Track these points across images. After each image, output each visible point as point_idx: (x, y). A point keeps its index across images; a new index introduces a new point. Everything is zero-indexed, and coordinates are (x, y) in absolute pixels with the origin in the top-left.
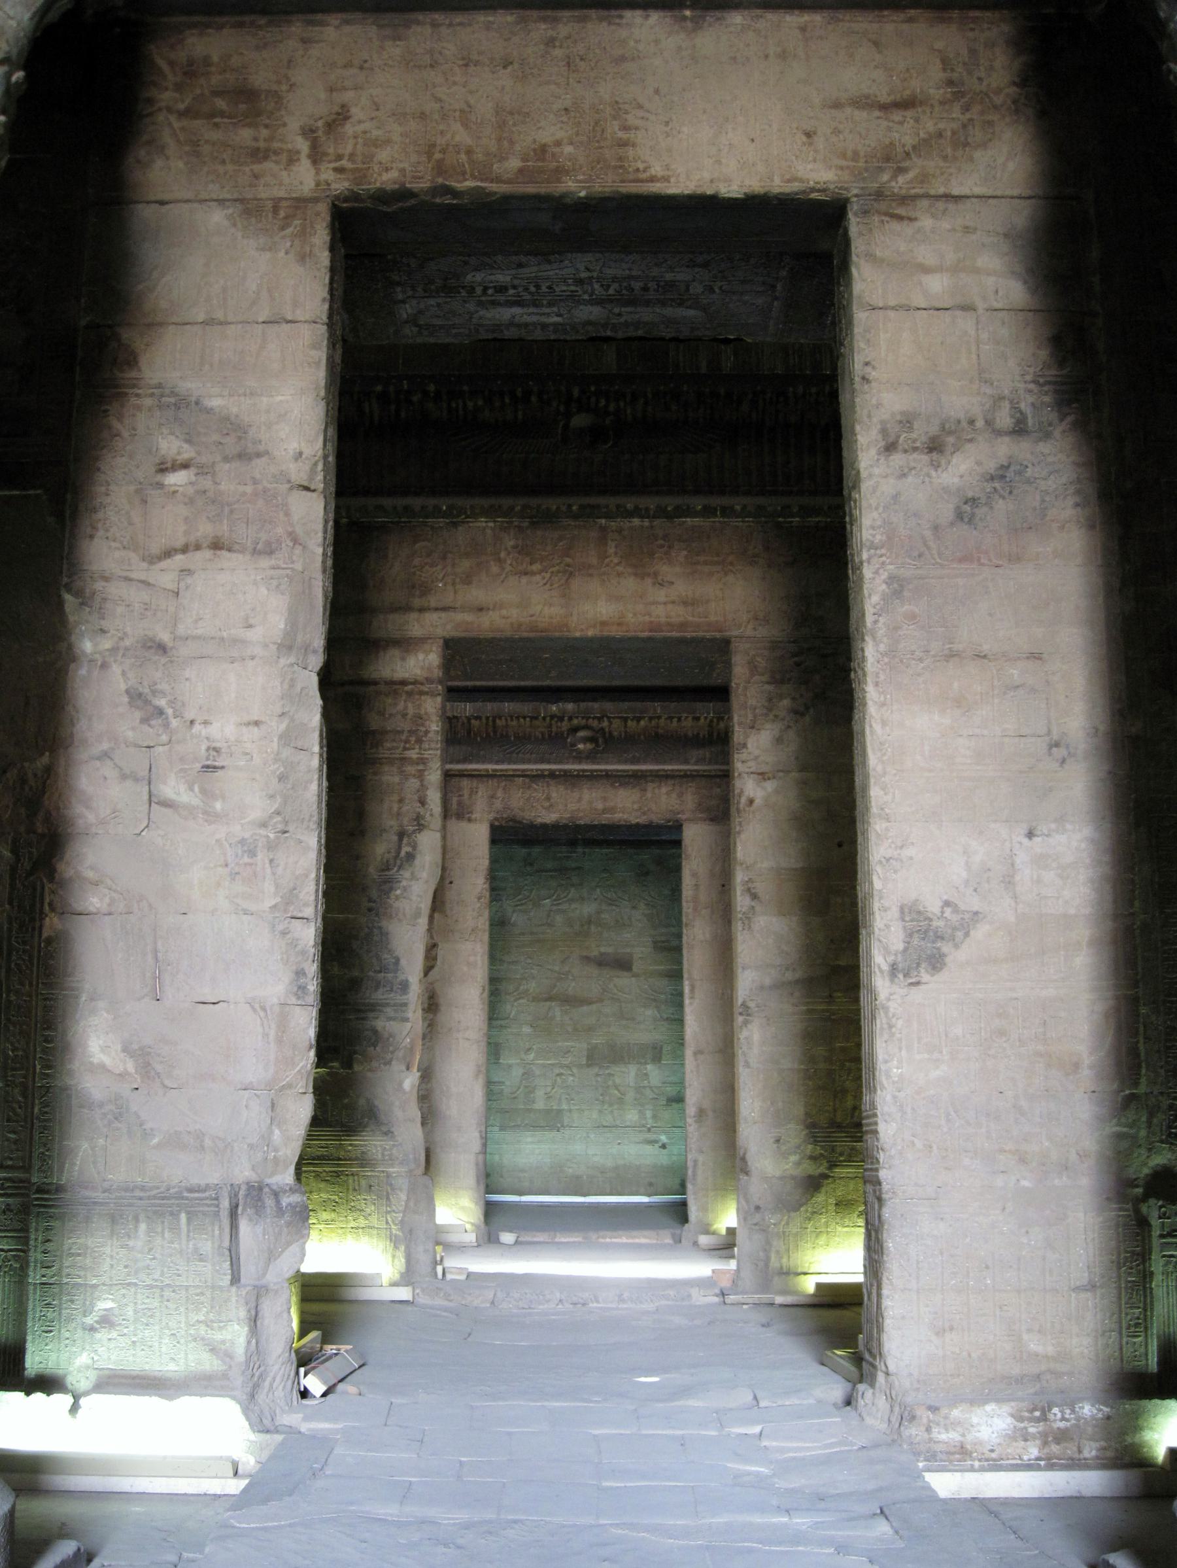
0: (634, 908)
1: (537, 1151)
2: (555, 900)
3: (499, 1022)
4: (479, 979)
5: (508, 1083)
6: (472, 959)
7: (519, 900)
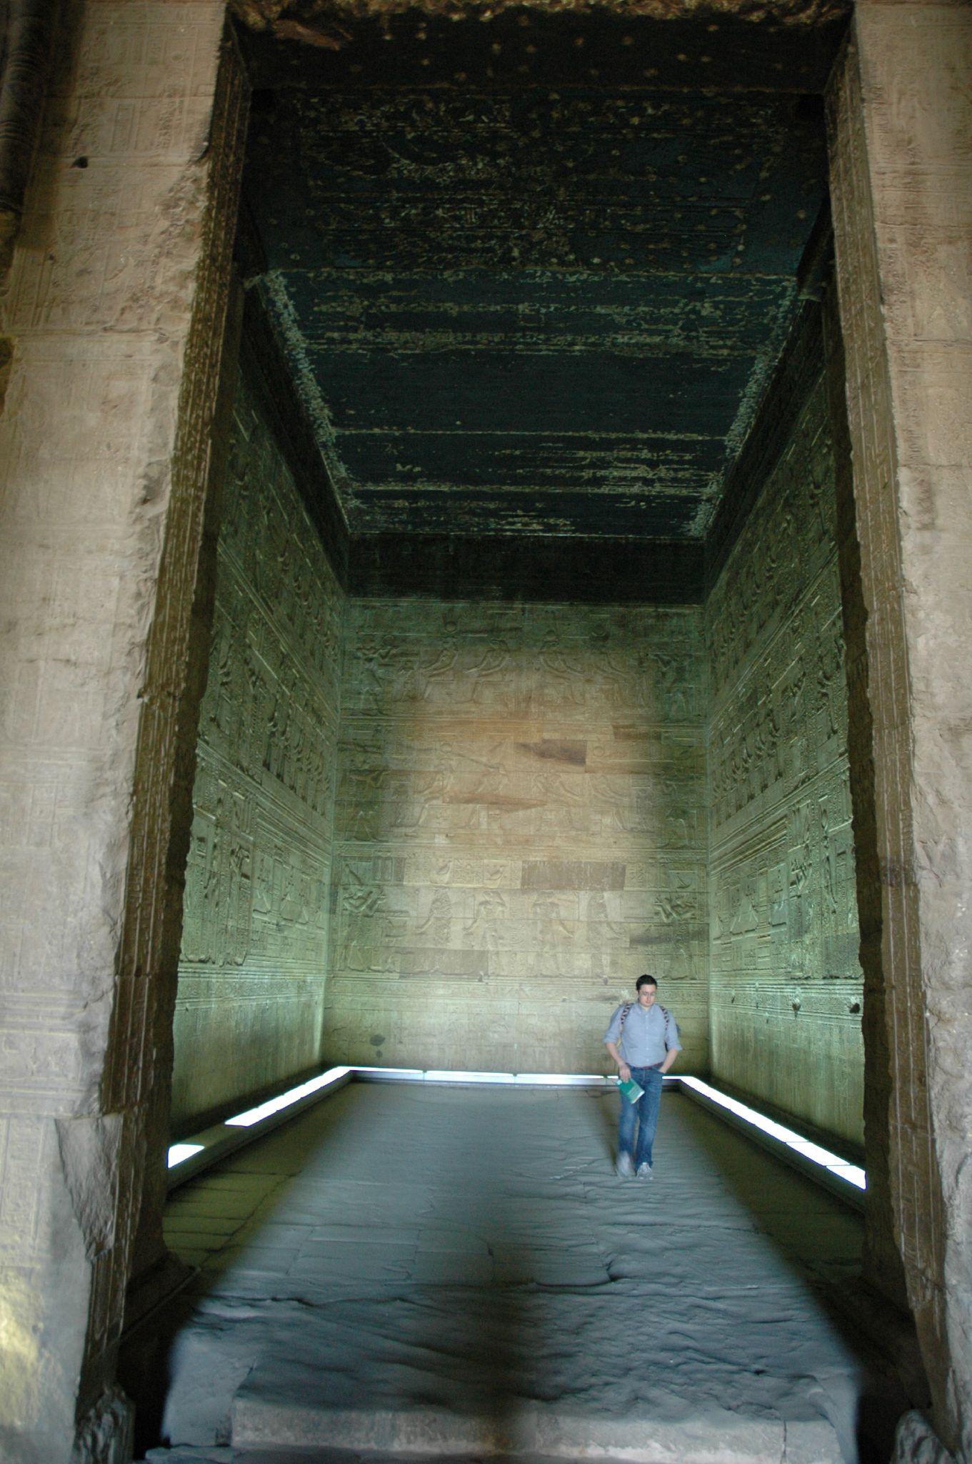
0: (588, 681)
1: (451, 1008)
2: (483, 670)
3: (403, 830)
4: (135, 453)
5: (413, 913)
6: (119, 387)
7: (435, 669)
